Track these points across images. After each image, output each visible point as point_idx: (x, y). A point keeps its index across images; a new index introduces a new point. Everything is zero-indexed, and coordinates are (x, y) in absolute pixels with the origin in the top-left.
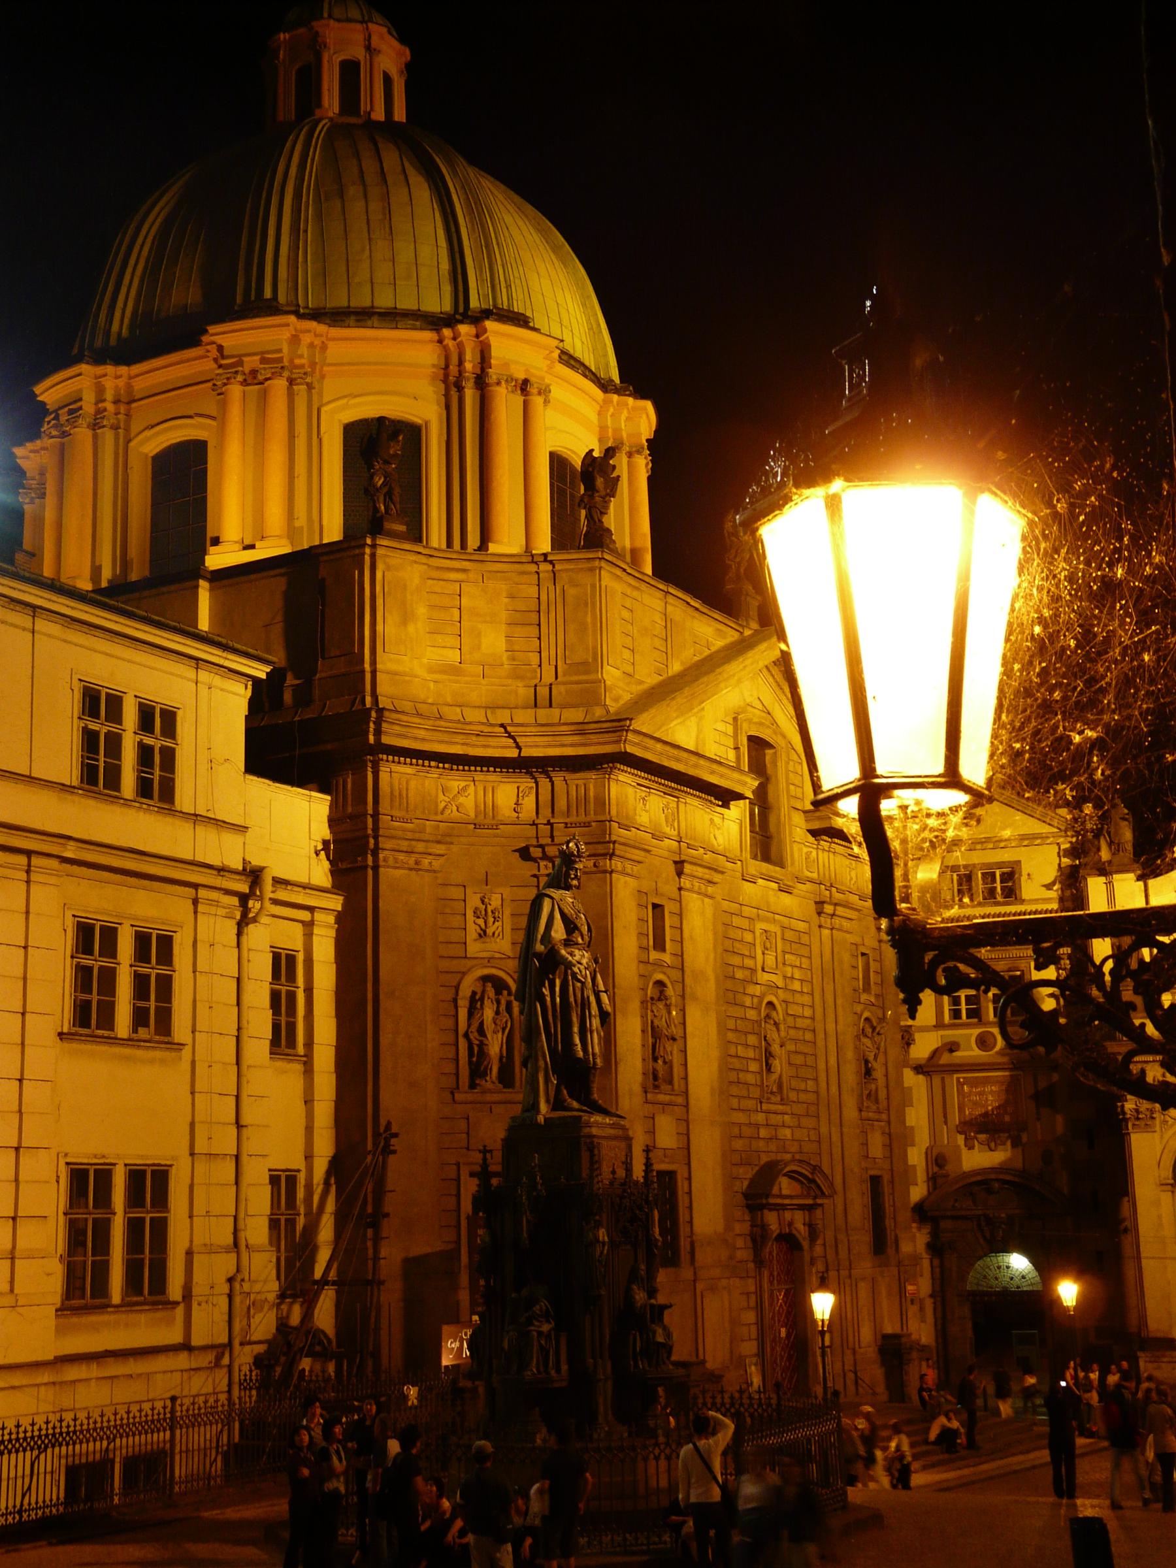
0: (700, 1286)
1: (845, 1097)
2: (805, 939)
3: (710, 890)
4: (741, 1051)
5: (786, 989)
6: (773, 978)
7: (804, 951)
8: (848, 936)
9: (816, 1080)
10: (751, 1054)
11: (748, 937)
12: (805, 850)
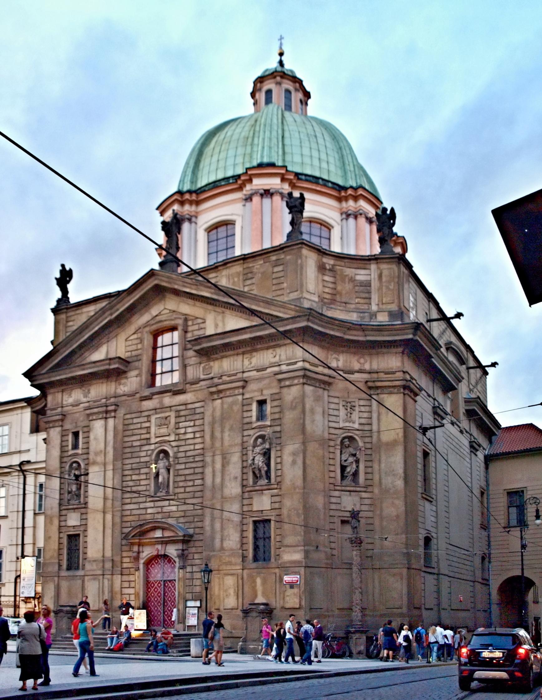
0: (86, 578)
1: (227, 483)
2: (202, 410)
3: (113, 414)
4: (134, 477)
5: (179, 440)
6: (167, 438)
7: (197, 417)
8: (240, 397)
9: (203, 479)
10: (144, 477)
11: (147, 425)
12: (202, 365)
